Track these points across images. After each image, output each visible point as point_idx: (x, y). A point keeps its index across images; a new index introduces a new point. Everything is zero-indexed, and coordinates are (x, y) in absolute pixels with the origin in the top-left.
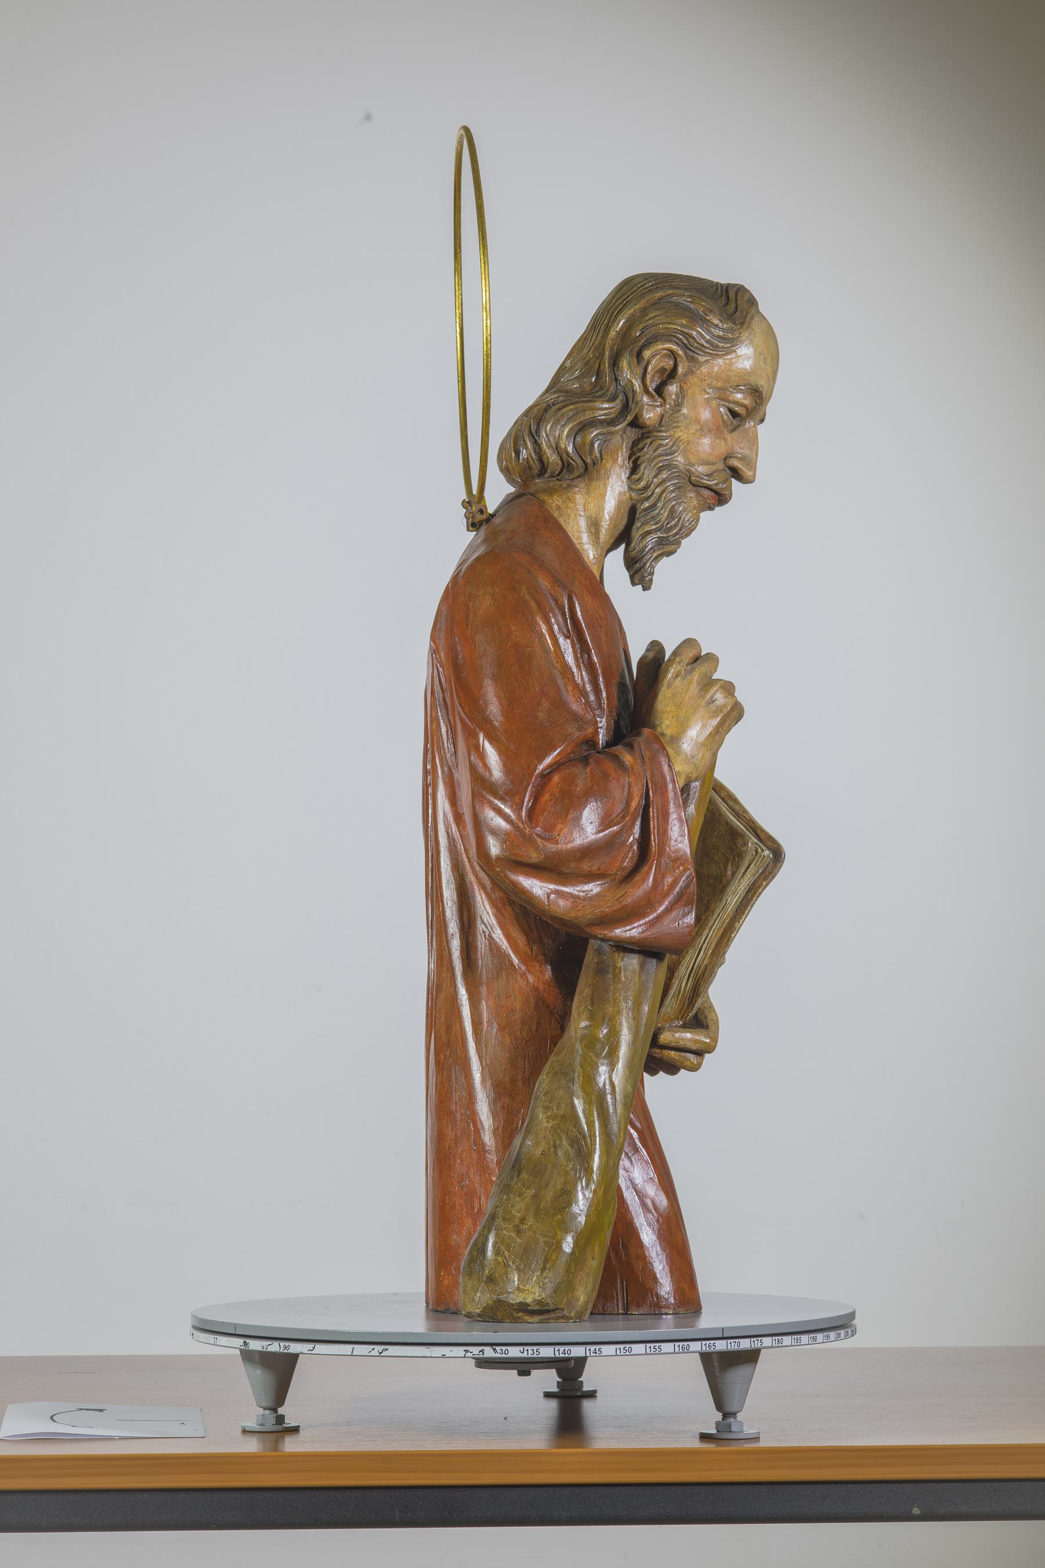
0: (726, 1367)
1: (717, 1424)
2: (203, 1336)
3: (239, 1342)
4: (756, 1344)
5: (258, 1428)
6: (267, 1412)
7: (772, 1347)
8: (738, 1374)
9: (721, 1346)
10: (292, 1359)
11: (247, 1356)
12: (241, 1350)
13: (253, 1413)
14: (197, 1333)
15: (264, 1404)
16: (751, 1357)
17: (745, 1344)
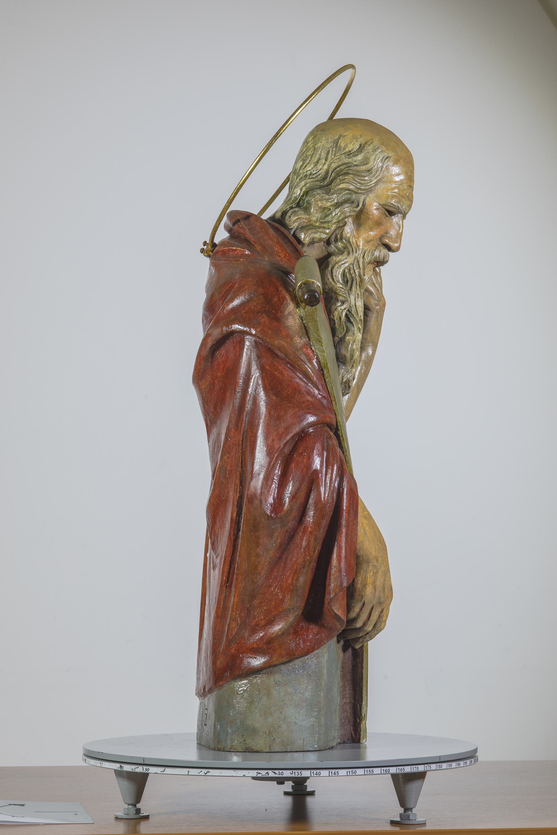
0: (407, 781)
2: (93, 762)
4: (427, 767)
6: (130, 807)
7: (436, 770)
8: (414, 785)
9: (408, 769)
11: (119, 774)
13: (121, 807)
14: (88, 759)
15: (129, 803)
16: (421, 776)
17: (421, 768)
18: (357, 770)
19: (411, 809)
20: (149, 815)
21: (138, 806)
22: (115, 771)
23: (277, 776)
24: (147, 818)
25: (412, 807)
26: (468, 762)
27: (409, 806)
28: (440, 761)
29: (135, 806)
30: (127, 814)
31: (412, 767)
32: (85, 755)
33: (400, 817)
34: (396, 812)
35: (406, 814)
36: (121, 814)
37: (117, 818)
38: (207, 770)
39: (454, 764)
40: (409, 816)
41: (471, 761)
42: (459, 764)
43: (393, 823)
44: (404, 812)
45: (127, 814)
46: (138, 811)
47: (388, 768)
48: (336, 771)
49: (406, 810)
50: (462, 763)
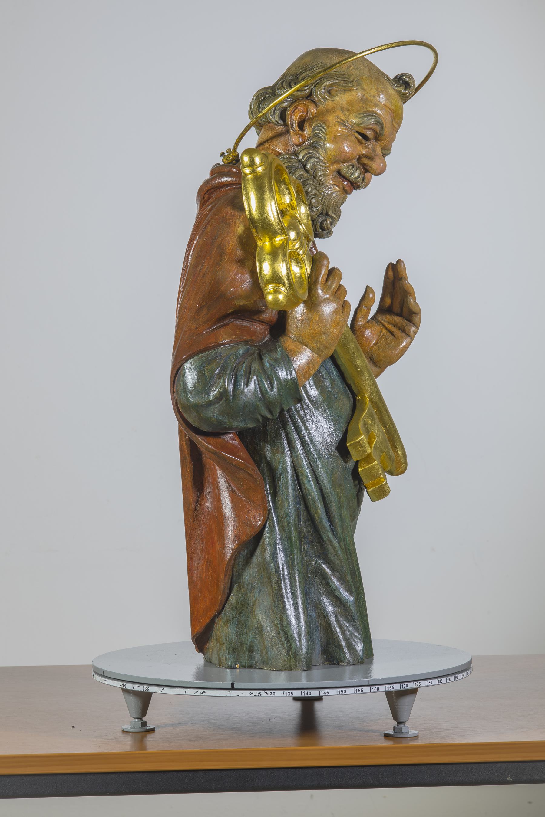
0: (398, 698)
1: (394, 728)
3: (119, 684)
5: (131, 730)
6: (137, 720)
7: (426, 686)
8: (406, 700)
9: (397, 687)
10: (151, 694)
11: (125, 691)
12: (122, 689)
16: (414, 691)
17: (411, 686)
18: (347, 689)
19: (404, 723)
20: (154, 728)
21: (144, 719)
22: (122, 689)
23: (269, 695)
24: (153, 730)
25: (404, 720)
26: (460, 676)
27: (402, 720)
28: (428, 678)
29: (141, 719)
30: (133, 728)
31: (401, 684)
32: (94, 671)
33: (394, 730)
34: (388, 725)
35: (399, 727)
36: (128, 727)
37: (124, 731)
38: (203, 690)
39: (444, 680)
40: (402, 729)
41: (463, 675)
42: (450, 679)
43: (387, 736)
44: (397, 725)
45: (133, 728)
46: (144, 724)
47: (377, 687)
48: (326, 690)
49: (399, 723)
50: (453, 678)
